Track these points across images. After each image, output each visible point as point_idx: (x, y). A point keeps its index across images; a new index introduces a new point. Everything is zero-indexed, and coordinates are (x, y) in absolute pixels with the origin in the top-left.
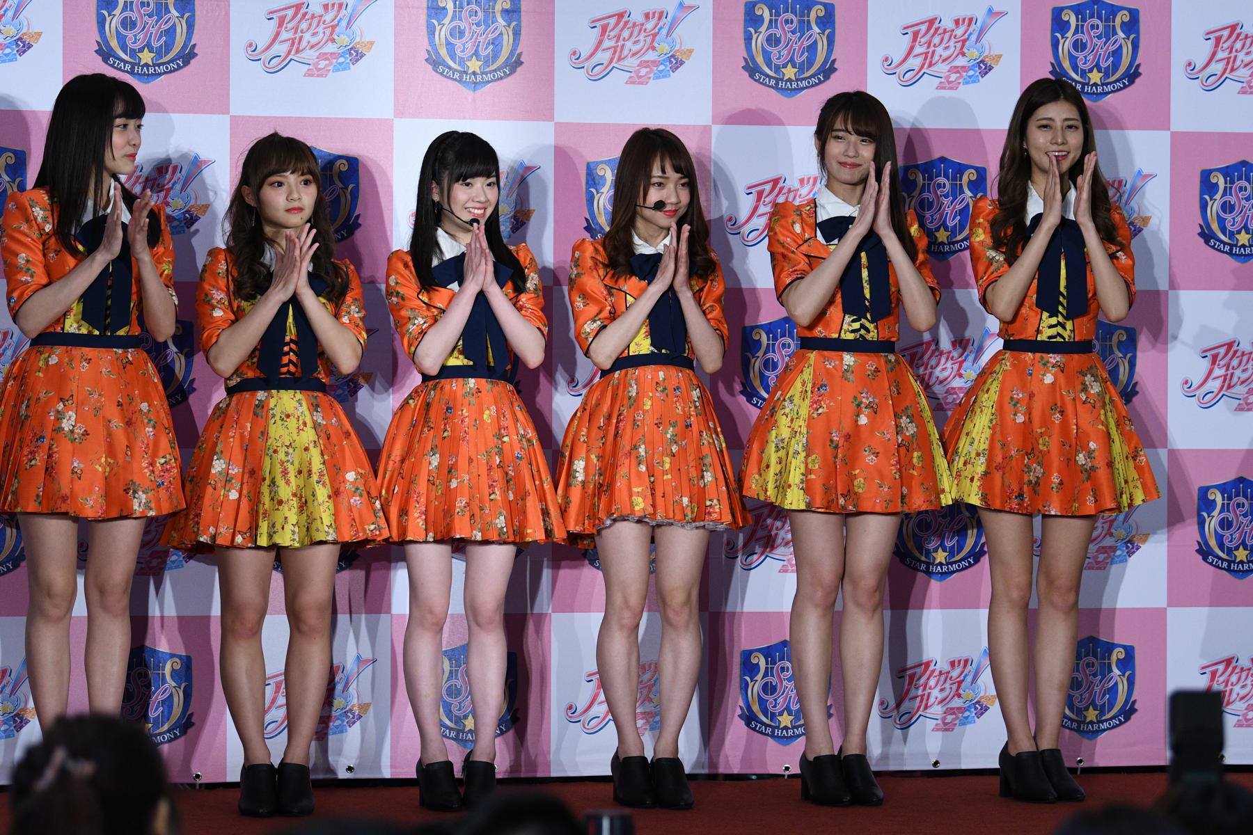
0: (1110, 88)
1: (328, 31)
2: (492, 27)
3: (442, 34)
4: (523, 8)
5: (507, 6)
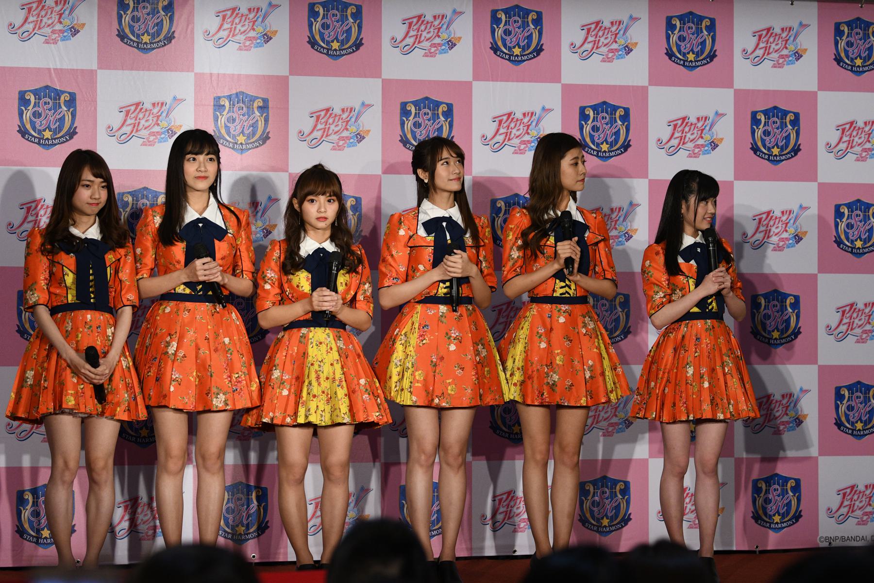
0: (784, 157)
1: (155, 119)
2: (252, 117)
3: (222, 120)
4: (270, 105)
5: (261, 104)
